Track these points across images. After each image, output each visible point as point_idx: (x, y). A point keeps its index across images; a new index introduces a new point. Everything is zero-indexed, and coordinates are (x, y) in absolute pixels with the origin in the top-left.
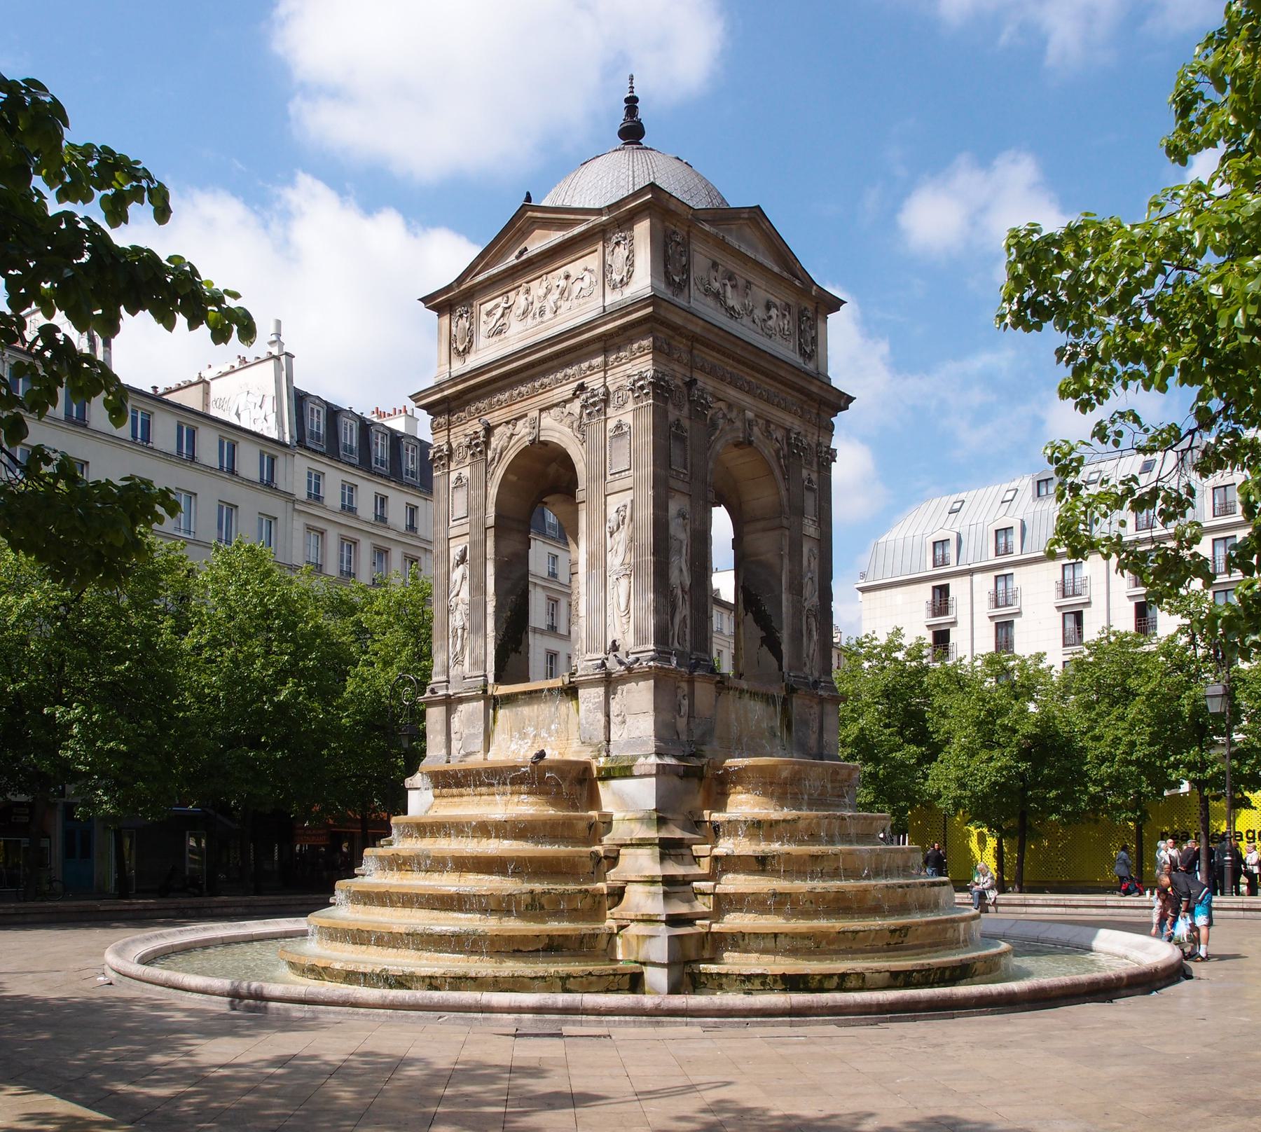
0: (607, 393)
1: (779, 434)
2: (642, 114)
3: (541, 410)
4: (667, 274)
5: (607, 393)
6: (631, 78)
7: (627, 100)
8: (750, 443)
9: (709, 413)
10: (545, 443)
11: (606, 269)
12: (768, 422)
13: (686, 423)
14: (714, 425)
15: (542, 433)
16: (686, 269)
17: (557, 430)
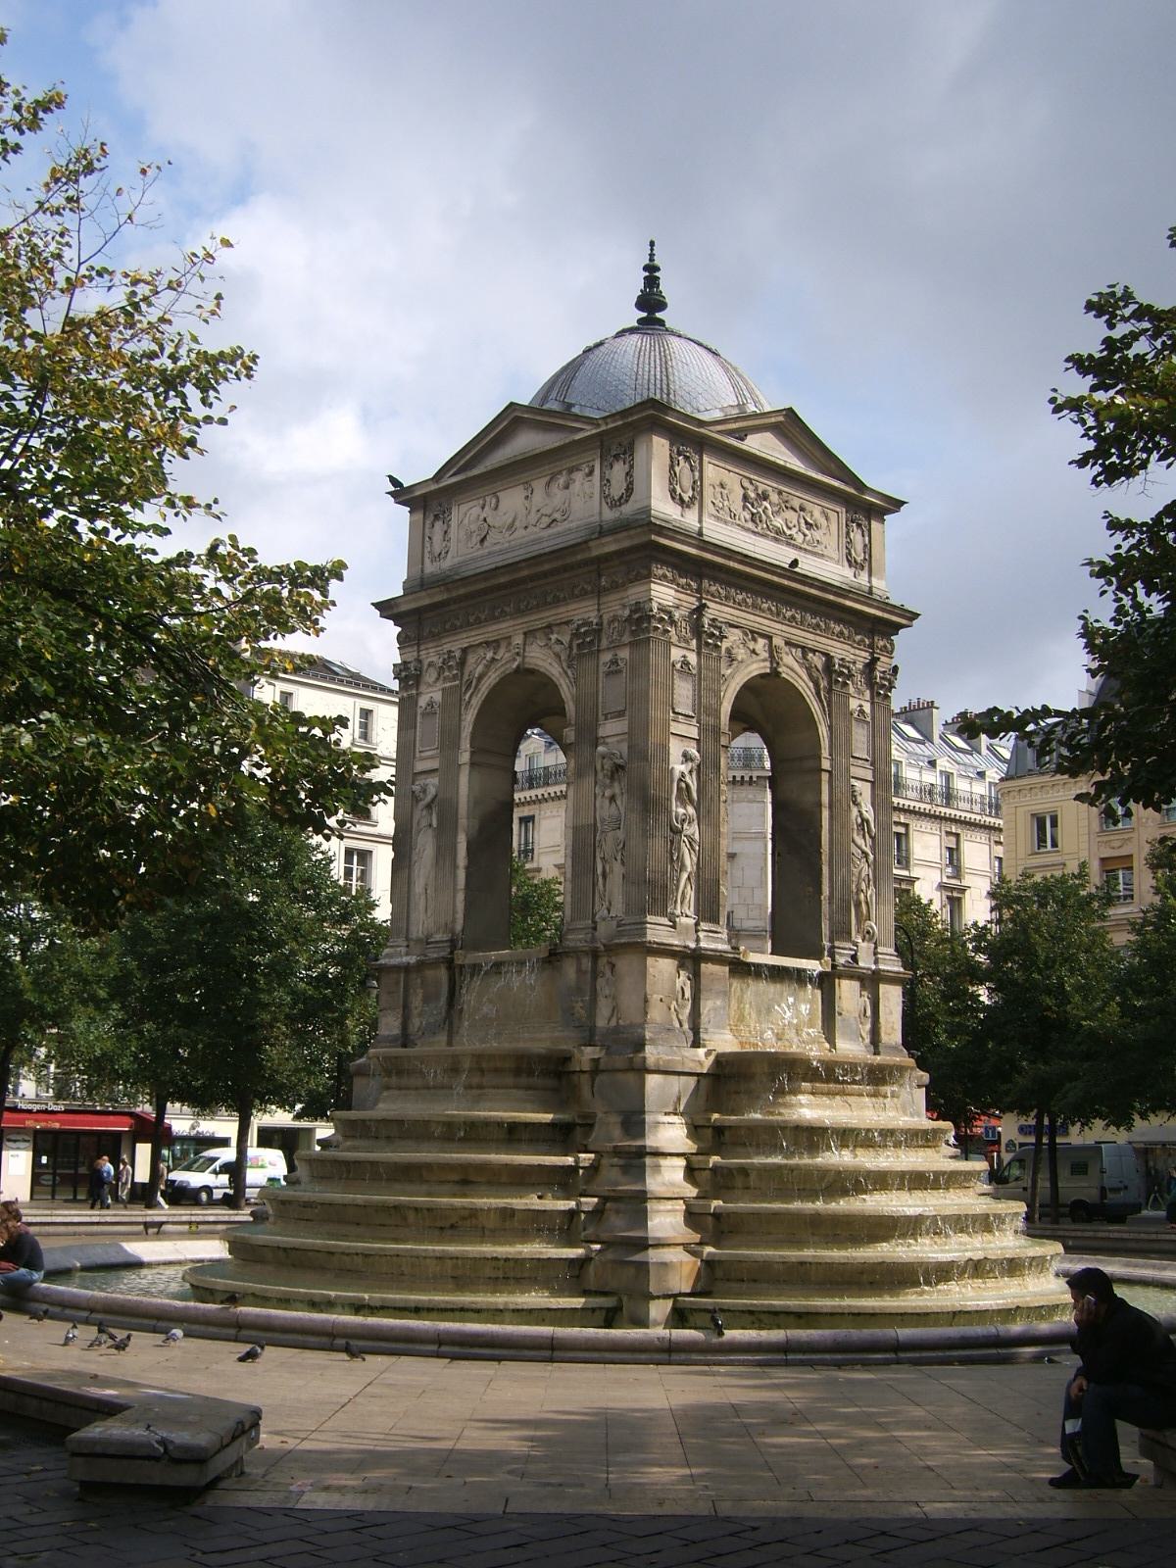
0: (600, 624)
1: (818, 661)
2: (667, 287)
3: (525, 634)
4: (673, 492)
5: (600, 624)
6: (652, 244)
7: (646, 268)
8: (778, 674)
9: (725, 645)
10: (532, 672)
11: (606, 482)
12: (805, 649)
13: (692, 658)
14: (731, 659)
15: (527, 660)
16: (698, 486)
17: (542, 658)
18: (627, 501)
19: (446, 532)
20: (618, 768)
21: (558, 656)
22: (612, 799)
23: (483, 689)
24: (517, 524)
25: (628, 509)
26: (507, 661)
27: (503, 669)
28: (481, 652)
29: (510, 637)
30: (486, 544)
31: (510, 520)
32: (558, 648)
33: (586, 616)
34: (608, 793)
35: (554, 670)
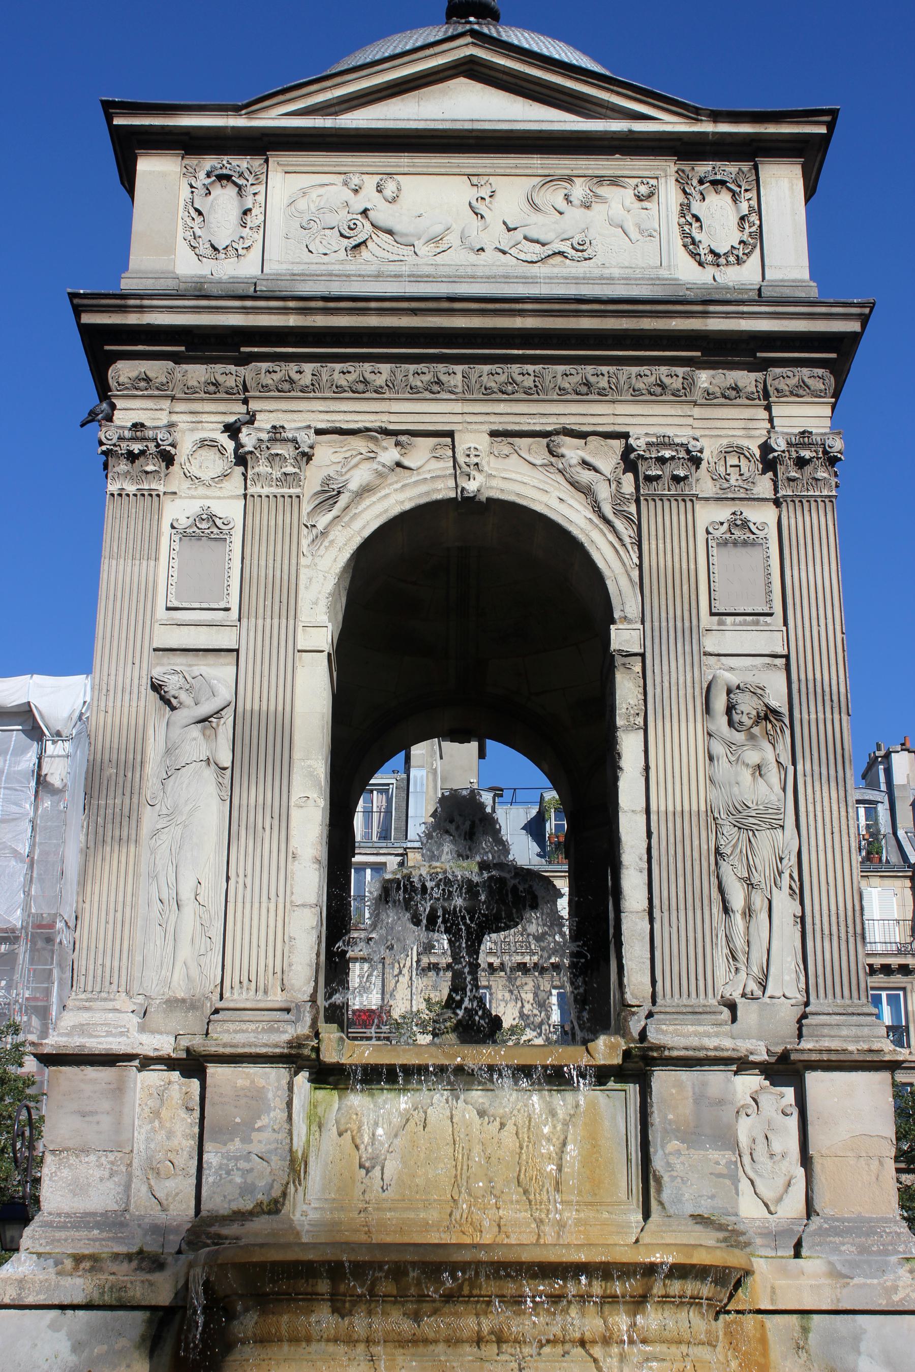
18: (739, 261)
19: (246, 212)
20: (769, 715)
21: (586, 491)
22: (759, 769)
23: (368, 516)
24: (453, 239)
25: (746, 275)
26: (425, 479)
27: (423, 488)
28: (359, 444)
29: (450, 434)
30: (365, 253)
31: (438, 229)
32: (586, 476)
33: (670, 432)
34: (752, 757)
35: (574, 516)
